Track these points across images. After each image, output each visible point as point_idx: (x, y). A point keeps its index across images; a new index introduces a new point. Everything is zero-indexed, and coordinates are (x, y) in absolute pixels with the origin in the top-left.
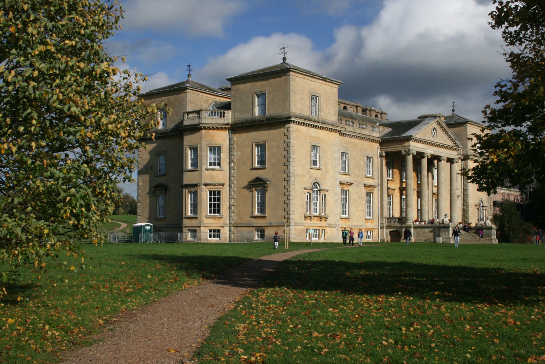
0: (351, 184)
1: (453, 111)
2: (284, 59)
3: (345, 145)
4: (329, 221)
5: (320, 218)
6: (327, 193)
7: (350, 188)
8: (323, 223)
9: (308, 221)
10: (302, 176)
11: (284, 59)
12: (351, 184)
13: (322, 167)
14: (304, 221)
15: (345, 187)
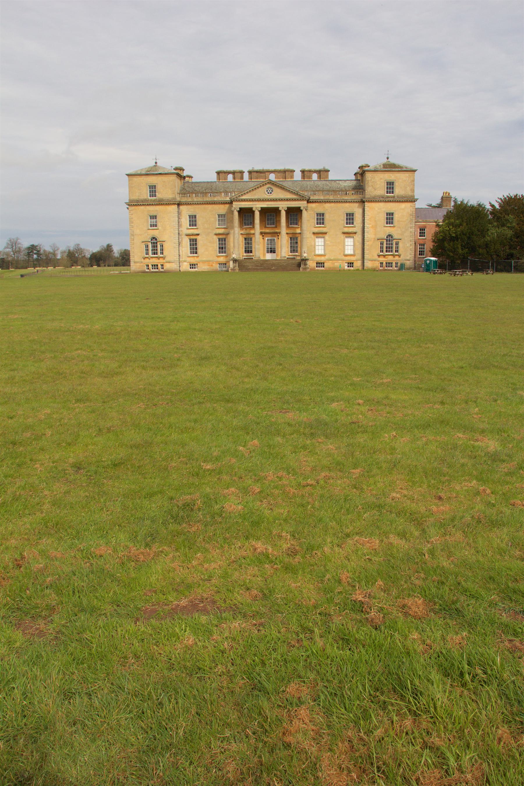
0: (198, 235)
1: (388, 158)
2: (156, 163)
3: (192, 210)
4: (167, 259)
5: (158, 258)
6: (163, 243)
7: (198, 238)
8: (161, 261)
9: (147, 260)
10: (140, 235)
11: (156, 163)
12: (198, 235)
13: (160, 228)
14: (143, 260)
15: (192, 237)
